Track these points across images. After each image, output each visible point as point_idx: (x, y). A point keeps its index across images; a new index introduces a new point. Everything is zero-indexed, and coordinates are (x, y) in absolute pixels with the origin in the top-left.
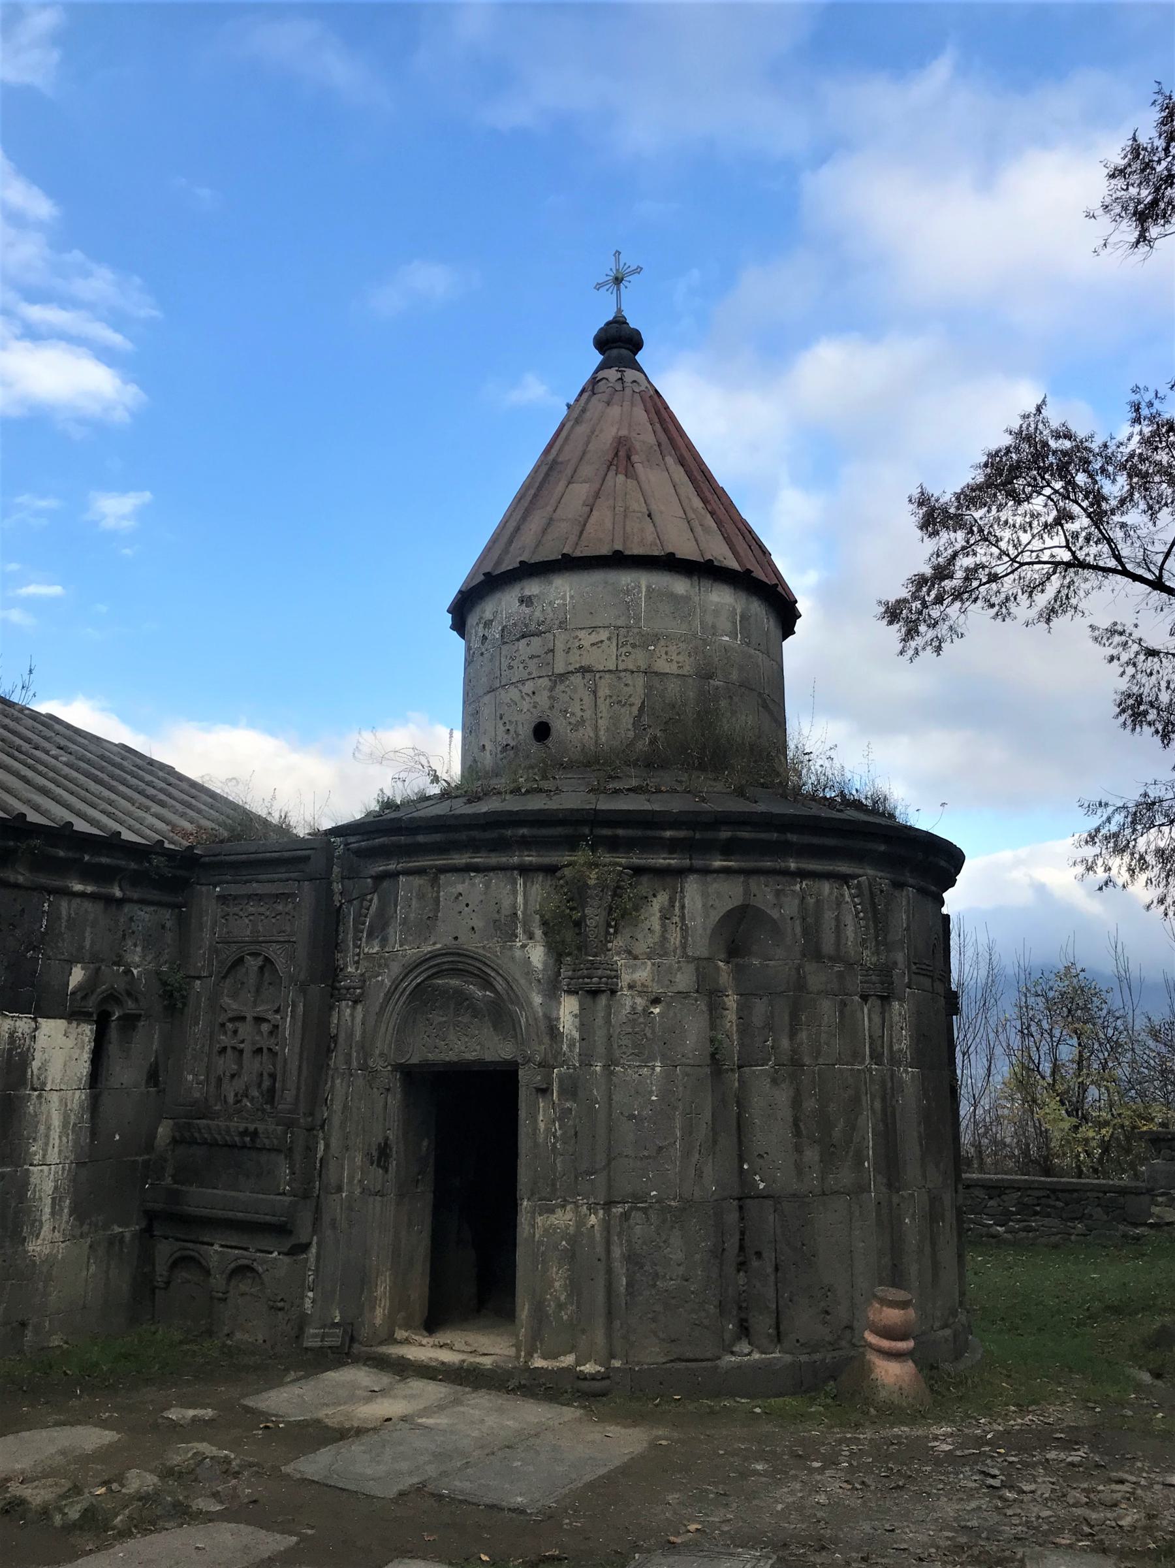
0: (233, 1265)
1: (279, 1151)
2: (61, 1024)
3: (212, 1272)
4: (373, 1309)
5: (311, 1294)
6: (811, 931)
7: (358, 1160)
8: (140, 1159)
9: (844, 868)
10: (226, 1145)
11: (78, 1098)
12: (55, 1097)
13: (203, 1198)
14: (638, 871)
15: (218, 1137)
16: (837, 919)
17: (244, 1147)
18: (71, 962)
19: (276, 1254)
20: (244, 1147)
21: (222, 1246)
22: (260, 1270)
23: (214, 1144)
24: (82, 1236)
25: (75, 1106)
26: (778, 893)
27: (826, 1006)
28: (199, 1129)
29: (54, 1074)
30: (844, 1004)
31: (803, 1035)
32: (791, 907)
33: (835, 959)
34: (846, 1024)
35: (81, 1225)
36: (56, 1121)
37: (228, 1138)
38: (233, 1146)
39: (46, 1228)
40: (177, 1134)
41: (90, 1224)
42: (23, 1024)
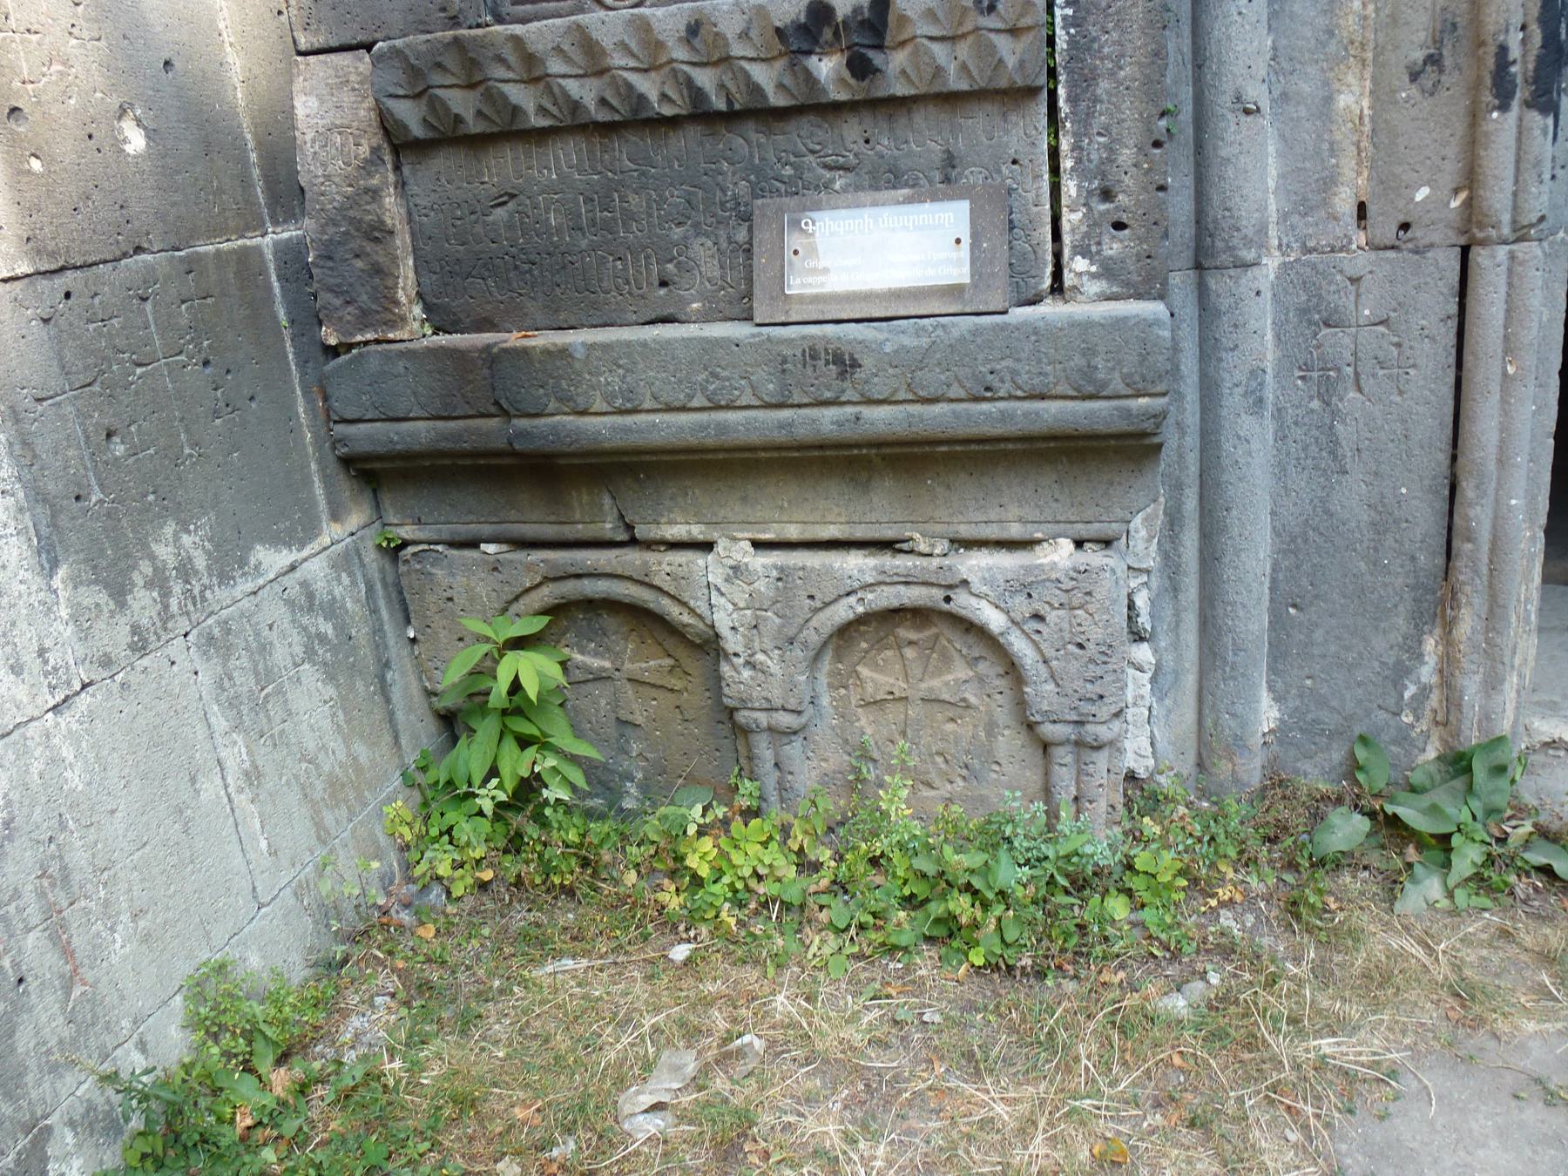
0: (844, 611)
1: (1020, 95)
3: (732, 643)
4: (1492, 684)
5: (1143, 653)
7: (1353, 98)
8: (268, 241)
10: (702, 116)
13: (628, 368)
15: (648, 86)
17: (814, 108)
19: (1066, 545)
20: (814, 108)
21: (757, 545)
22: (994, 620)
23: (638, 121)
24: (140, 645)
28: (530, 60)
35: (120, 593)
37: (705, 79)
38: (756, 113)
40: (409, 114)
41: (159, 582)
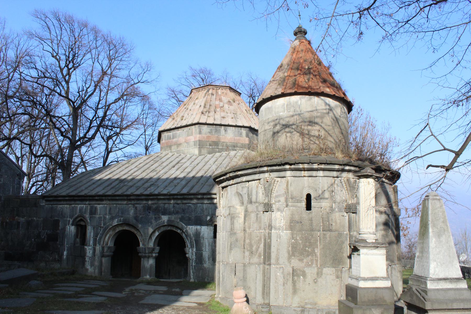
2: (206, 227)
6: (249, 195)
9: (256, 177)
11: (211, 240)
12: (206, 240)
14: (223, 188)
16: (257, 191)
18: (207, 216)
25: (211, 241)
26: (242, 188)
27: (253, 216)
29: (206, 236)
30: (257, 214)
31: (246, 224)
32: (245, 190)
33: (256, 202)
34: (258, 219)
36: (207, 244)
39: (207, 262)
42: (198, 227)
